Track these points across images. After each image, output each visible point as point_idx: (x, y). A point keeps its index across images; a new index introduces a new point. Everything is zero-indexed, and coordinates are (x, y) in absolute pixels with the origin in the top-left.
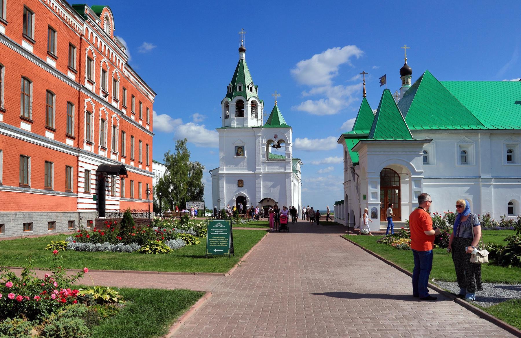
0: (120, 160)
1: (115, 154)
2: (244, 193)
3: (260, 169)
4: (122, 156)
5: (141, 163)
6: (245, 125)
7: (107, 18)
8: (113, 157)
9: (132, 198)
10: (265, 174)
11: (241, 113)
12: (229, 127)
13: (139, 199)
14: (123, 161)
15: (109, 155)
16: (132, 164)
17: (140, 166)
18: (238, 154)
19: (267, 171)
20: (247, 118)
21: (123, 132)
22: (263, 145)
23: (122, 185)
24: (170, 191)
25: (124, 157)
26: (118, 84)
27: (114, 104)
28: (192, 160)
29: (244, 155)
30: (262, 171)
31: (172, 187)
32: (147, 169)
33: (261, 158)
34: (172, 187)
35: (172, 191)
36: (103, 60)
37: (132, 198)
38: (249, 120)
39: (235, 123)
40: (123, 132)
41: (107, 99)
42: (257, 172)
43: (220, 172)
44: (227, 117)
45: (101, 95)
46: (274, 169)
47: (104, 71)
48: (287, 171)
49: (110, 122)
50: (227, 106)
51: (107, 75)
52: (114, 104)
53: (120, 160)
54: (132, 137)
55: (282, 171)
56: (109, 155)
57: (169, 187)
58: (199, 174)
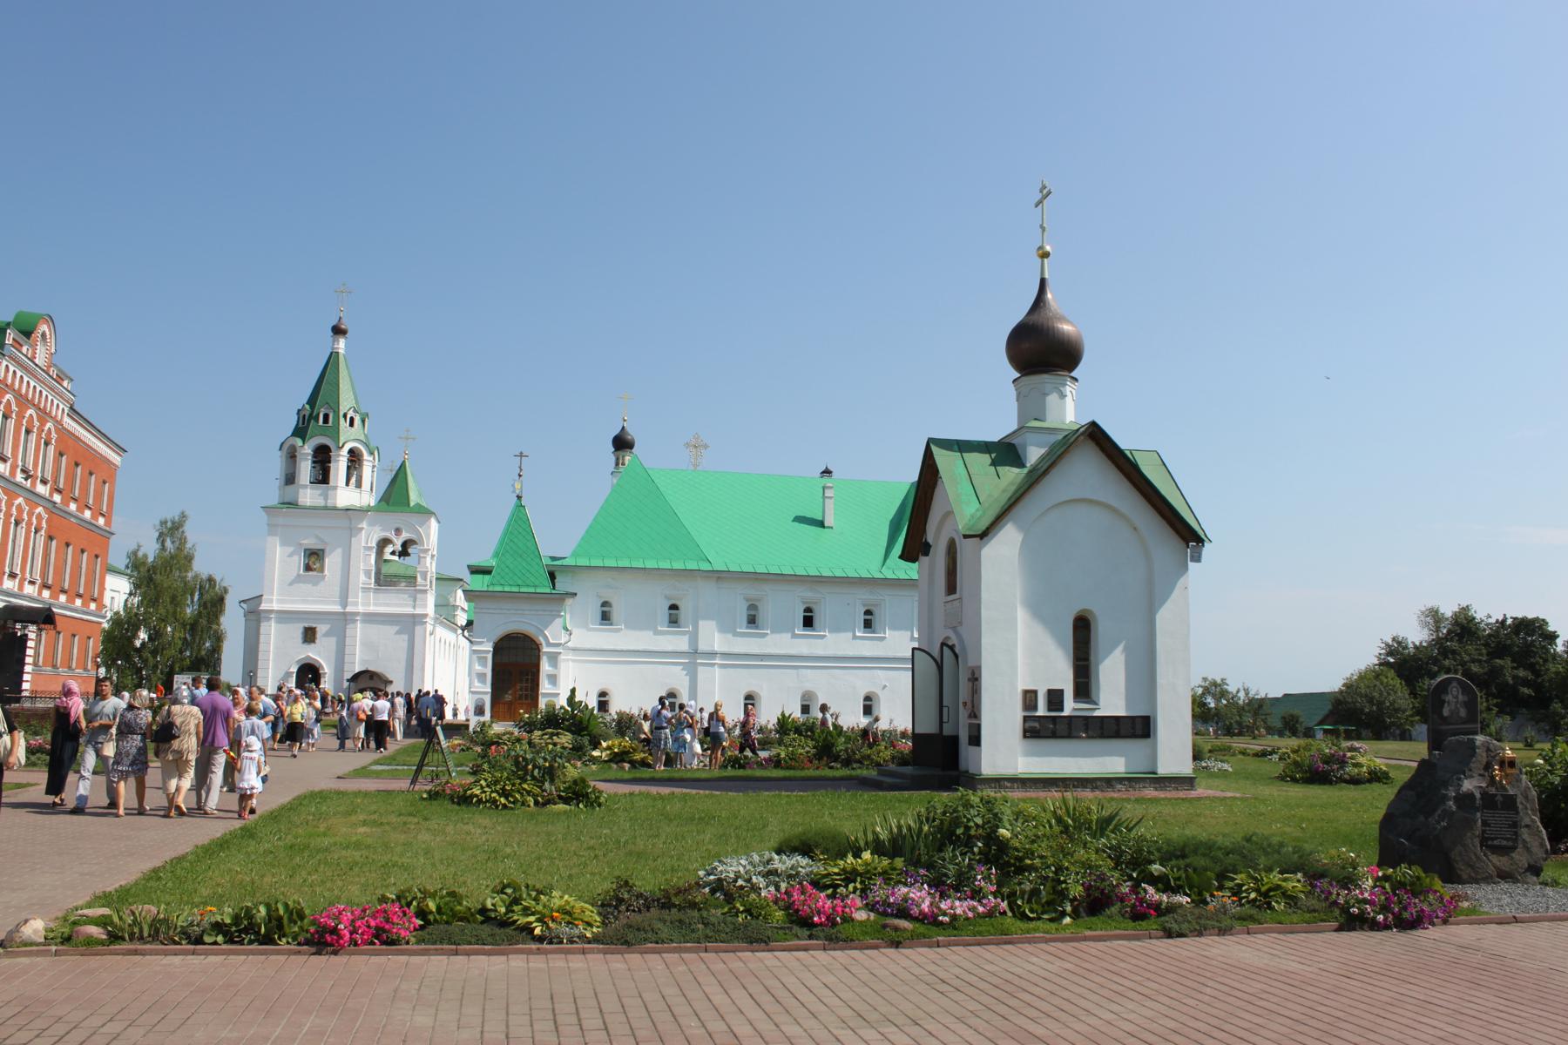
0: (40, 593)
1: (32, 583)
2: (315, 653)
3: (356, 604)
4: (45, 586)
5: (80, 596)
6: (330, 503)
7: (44, 335)
8: (29, 589)
9: (54, 666)
10: (365, 614)
11: (323, 476)
12: (292, 504)
13: (70, 668)
14: (46, 594)
15: (21, 586)
16: (63, 598)
17: (78, 602)
18: (308, 568)
19: (372, 609)
20: (335, 488)
21: (51, 538)
22: (370, 548)
23: (38, 641)
24: (138, 644)
25: (48, 587)
26: (51, 449)
27: (41, 489)
28: (201, 567)
29: (322, 570)
30: (361, 609)
31: (143, 635)
32: (93, 606)
33: (362, 578)
34: (143, 635)
35: (143, 644)
36: (30, 412)
37: (54, 666)
38: (339, 491)
39: (309, 495)
40: (51, 538)
41: (28, 484)
42: (348, 609)
43: (264, 606)
44: (290, 479)
45: (19, 477)
46: (388, 605)
47: (28, 432)
48: (418, 611)
49: (29, 524)
50: (292, 456)
51: (33, 436)
52: (41, 489)
53: (40, 593)
54: (68, 545)
55: (409, 610)
56: (21, 586)
57: (135, 636)
58: (214, 604)
